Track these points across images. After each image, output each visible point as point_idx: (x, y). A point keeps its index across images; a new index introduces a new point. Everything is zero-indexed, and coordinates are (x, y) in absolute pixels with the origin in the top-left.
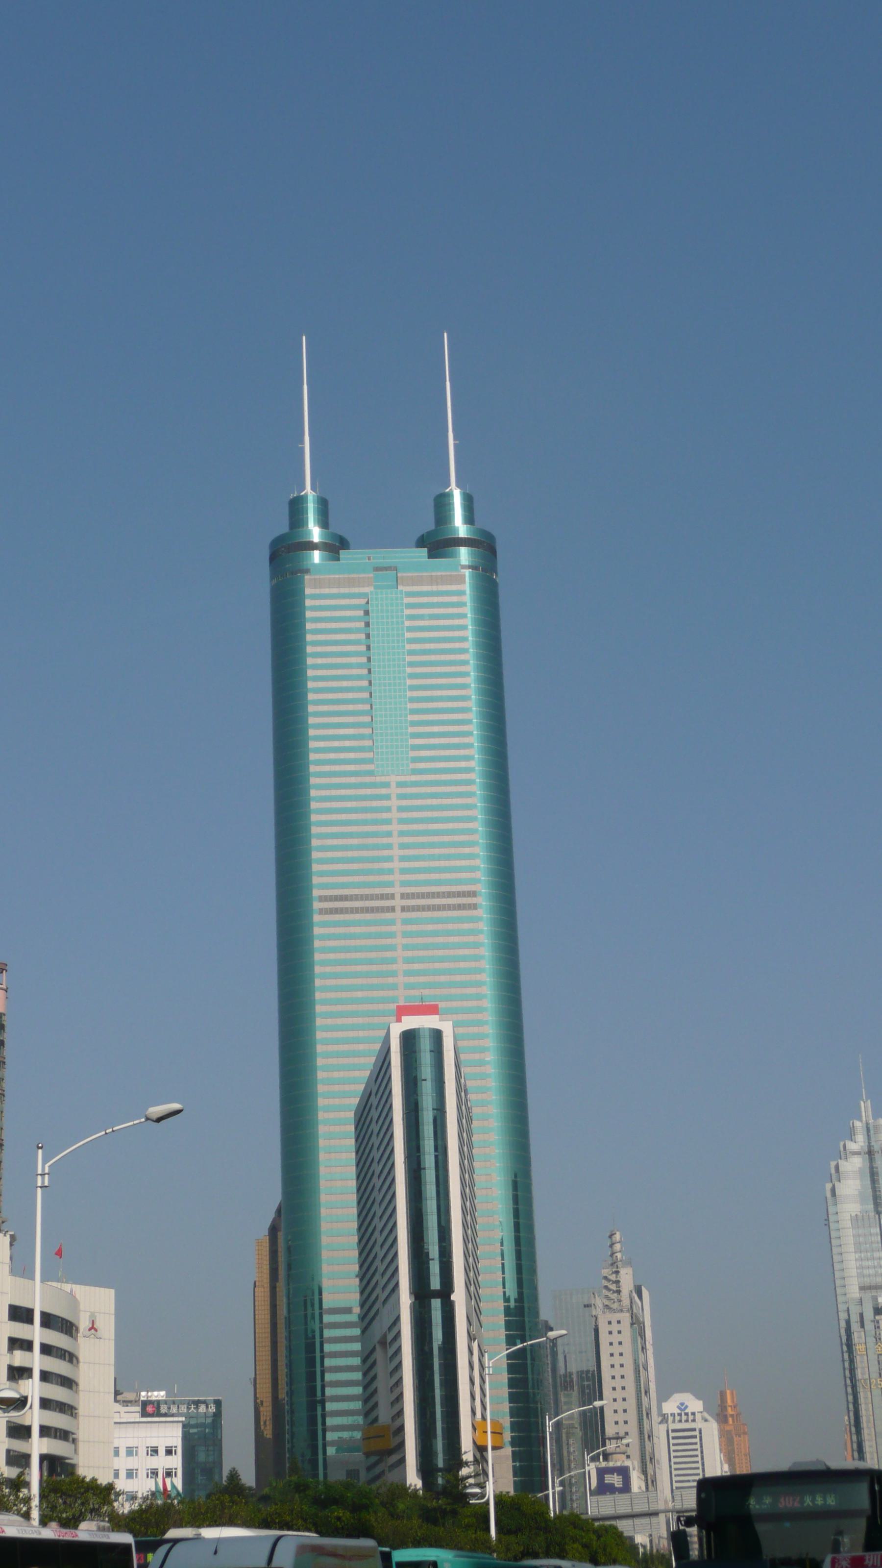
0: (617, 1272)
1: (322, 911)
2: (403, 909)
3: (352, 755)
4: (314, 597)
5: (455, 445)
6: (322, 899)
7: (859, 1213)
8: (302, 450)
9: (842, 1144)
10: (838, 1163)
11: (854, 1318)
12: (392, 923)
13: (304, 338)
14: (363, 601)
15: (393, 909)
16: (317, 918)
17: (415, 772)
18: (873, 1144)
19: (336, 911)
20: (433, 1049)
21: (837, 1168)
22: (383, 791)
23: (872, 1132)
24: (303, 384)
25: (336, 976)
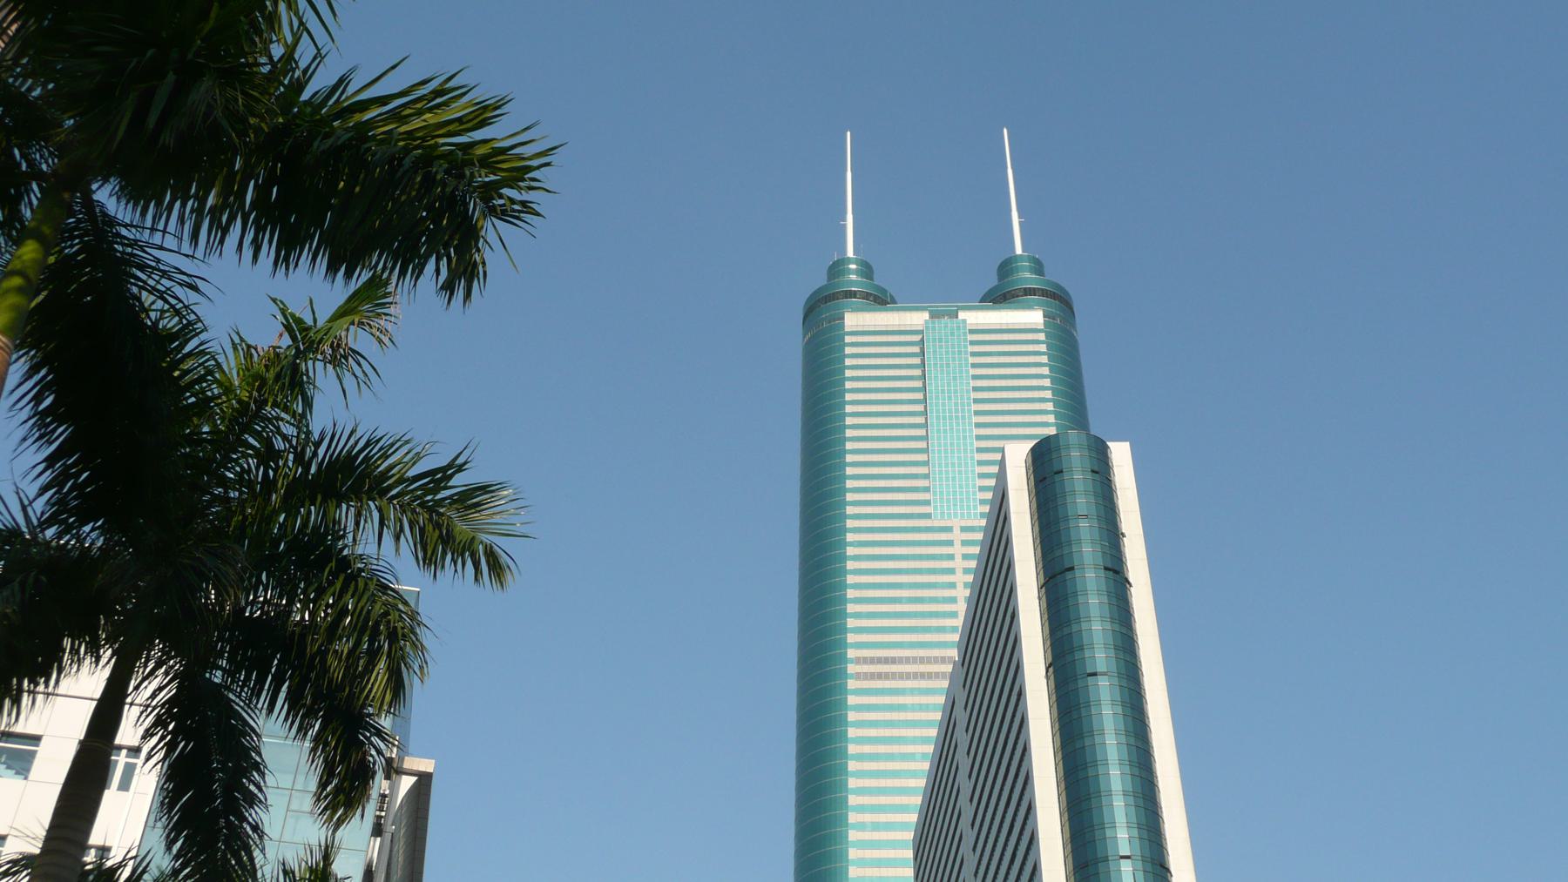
1: (858, 676)
5: (1020, 222)
6: (858, 661)
8: (844, 227)
13: (849, 133)
14: (916, 349)
16: (852, 684)
19: (880, 676)
20: (1096, 469)
22: (943, 536)
24: (846, 170)
25: (876, 827)
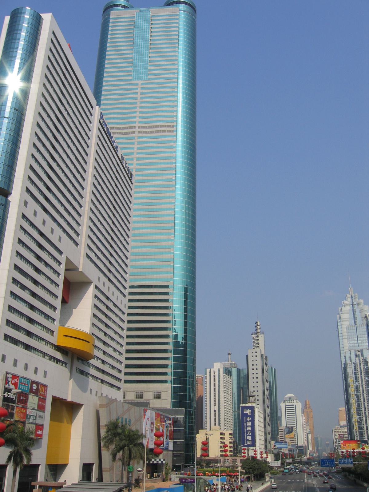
0: (258, 336)
2: (139, 132)
3: (123, 74)
4: (113, 19)
7: (349, 325)
9: (343, 302)
10: (341, 309)
11: (348, 359)
12: (134, 138)
15: (134, 133)
17: (150, 79)
18: (353, 301)
21: (341, 310)
23: (353, 298)
